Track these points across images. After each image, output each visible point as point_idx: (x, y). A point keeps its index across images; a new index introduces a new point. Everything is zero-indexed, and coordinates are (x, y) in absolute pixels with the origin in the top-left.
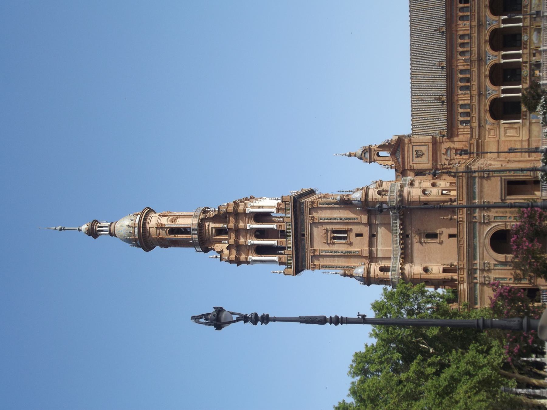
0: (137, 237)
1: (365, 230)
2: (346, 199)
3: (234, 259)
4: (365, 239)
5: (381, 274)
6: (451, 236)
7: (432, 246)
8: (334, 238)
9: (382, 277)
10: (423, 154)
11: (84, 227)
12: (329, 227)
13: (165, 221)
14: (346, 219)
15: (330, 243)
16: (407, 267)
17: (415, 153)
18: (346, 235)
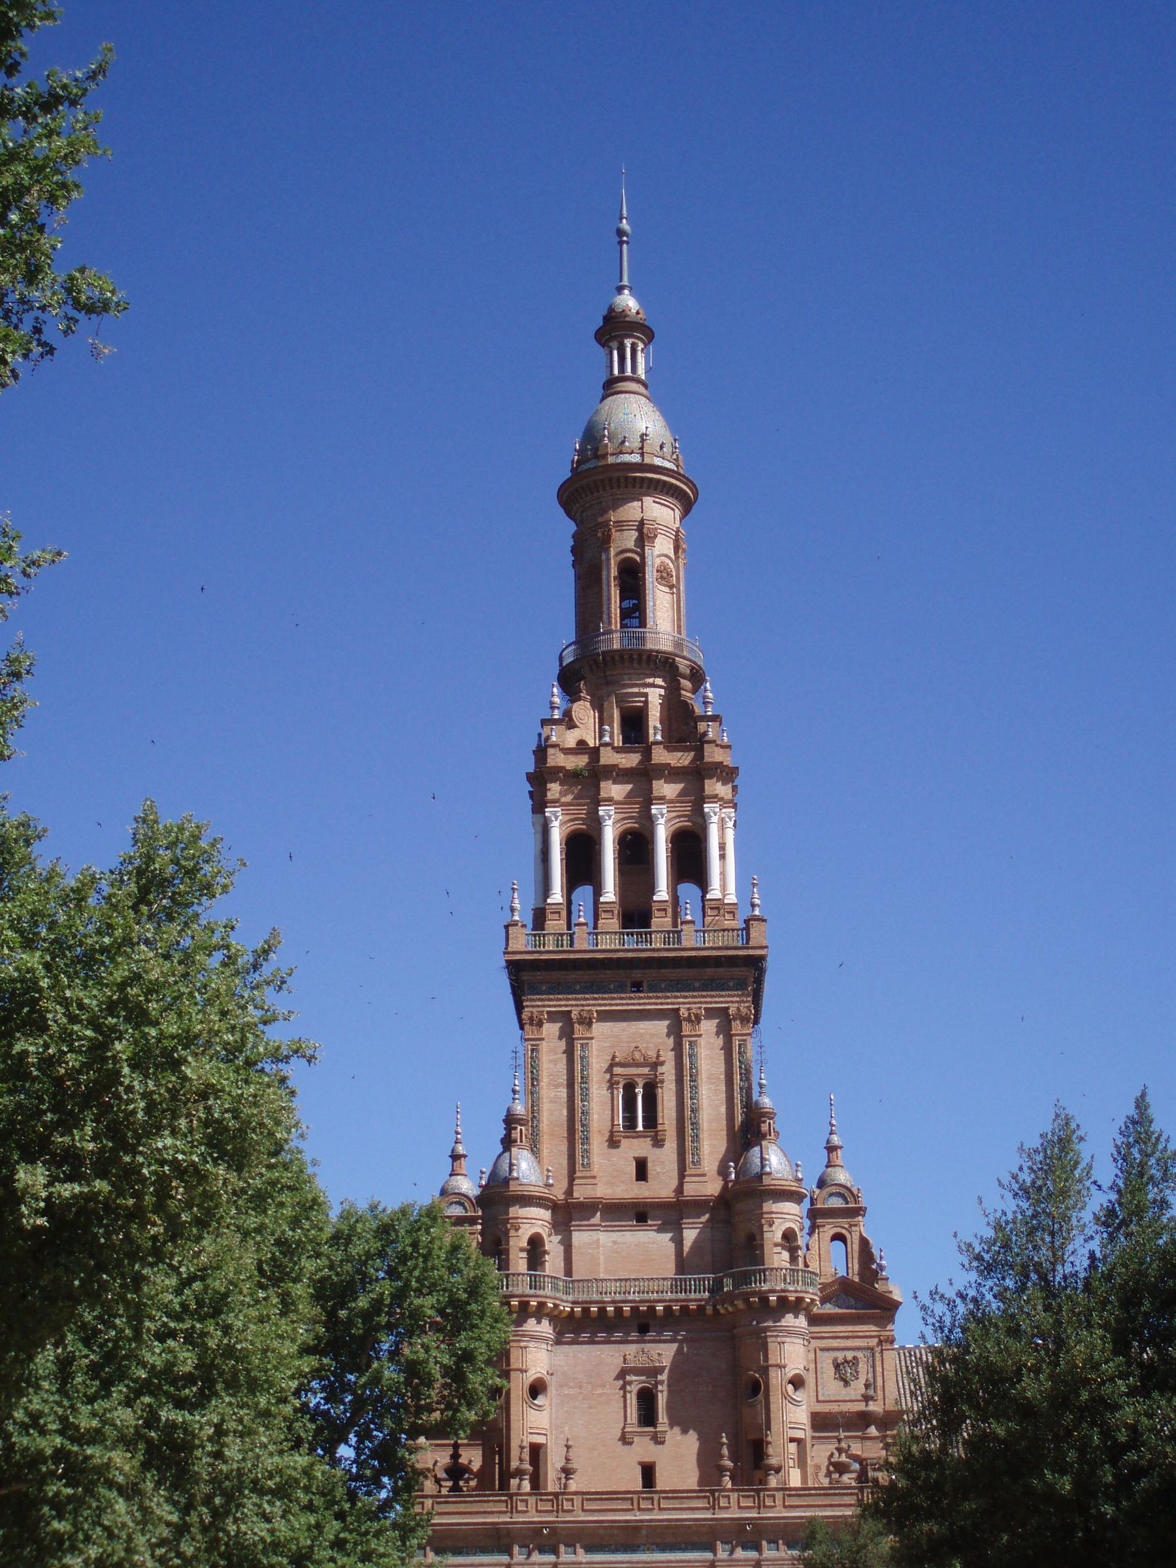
0: (611, 460)
1: (661, 1186)
2: (764, 1128)
3: (551, 762)
4: (628, 1190)
5: (519, 1242)
6: (648, 1472)
7: (617, 1410)
8: (629, 1089)
9: (512, 1242)
10: (847, 1383)
11: (629, 302)
12: (668, 1071)
13: (661, 549)
14: (695, 1125)
15: (612, 1075)
16: (546, 1328)
17: (850, 1355)
18: (640, 1128)
